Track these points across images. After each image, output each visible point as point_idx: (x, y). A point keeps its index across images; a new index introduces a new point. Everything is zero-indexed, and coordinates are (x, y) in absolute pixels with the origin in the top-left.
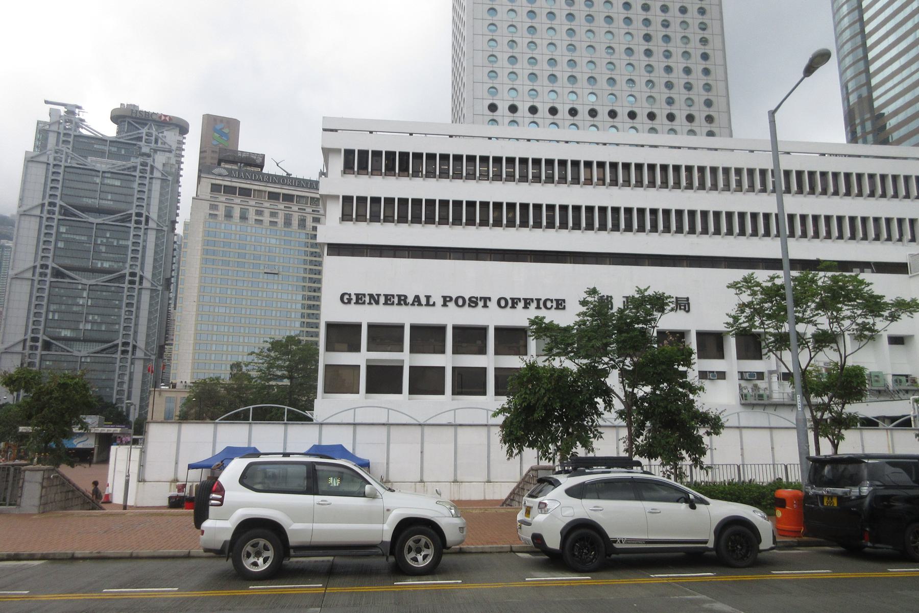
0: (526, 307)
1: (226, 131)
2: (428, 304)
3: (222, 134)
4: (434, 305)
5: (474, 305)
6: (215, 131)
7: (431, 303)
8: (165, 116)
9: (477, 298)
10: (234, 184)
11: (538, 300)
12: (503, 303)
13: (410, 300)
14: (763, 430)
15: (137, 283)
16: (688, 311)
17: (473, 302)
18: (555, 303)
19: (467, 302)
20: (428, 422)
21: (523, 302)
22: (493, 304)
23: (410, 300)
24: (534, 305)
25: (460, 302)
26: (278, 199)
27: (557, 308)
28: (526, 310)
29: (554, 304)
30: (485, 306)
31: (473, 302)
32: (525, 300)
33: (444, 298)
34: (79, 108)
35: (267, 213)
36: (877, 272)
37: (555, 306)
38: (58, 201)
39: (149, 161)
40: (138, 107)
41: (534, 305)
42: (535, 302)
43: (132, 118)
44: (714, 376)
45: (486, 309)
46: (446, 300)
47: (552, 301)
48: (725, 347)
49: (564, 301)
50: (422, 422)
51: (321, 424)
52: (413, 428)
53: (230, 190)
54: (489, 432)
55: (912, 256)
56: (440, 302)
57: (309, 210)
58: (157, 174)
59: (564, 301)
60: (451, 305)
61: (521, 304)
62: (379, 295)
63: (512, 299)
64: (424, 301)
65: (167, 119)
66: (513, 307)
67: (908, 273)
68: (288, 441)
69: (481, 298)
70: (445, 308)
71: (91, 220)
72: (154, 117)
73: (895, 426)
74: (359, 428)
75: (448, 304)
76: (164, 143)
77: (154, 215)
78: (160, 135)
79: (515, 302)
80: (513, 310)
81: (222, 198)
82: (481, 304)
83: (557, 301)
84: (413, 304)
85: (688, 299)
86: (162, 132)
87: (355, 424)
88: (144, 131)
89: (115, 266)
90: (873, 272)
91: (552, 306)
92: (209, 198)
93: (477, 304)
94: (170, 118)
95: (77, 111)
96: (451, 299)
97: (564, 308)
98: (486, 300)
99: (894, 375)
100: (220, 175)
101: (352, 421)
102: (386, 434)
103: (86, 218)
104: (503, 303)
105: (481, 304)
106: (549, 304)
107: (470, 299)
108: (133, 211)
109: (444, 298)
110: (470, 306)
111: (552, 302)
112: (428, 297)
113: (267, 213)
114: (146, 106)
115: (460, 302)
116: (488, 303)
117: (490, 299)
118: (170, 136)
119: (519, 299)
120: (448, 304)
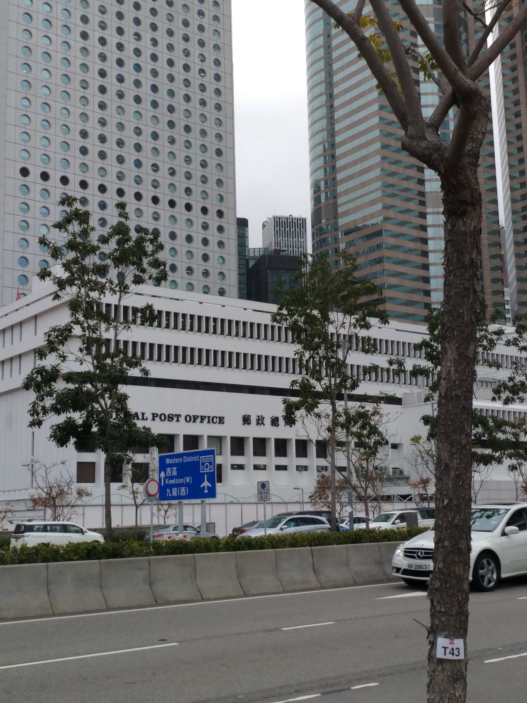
0: (201, 422)
2: (143, 419)
4: (147, 419)
5: (171, 420)
7: (145, 418)
9: (173, 415)
11: (209, 417)
12: (188, 419)
14: (281, 504)
17: (170, 418)
18: (218, 419)
19: (167, 418)
20: (289, 501)
21: (200, 418)
22: (182, 419)
24: (206, 420)
25: (163, 418)
27: (220, 423)
28: (202, 424)
29: (218, 420)
30: (178, 421)
31: (170, 418)
32: (201, 417)
33: (153, 414)
36: (387, 403)
37: (218, 422)
41: (206, 420)
42: (207, 418)
44: (302, 469)
45: (178, 423)
46: (154, 416)
47: (216, 418)
48: (308, 449)
49: (223, 418)
50: (286, 501)
51: (242, 503)
52: (188, 506)
54: (272, 506)
55: (405, 394)
56: (150, 417)
59: (223, 418)
60: (157, 419)
61: (199, 420)
63: (194, 416)
64: (140, 416)
66: (194, 421)
67: (401, 405)
68: (124, 516)
69: (175, 415)
70: (154, 421)
73: (408, 500)
74: (124, 508)
75: (155, 418)
79: (195, 418)
80: (194, 424)
82: (175, 419)
83: (220, 418)
87: (122, 505)
90: (385, 403)
93: (173, 419)
96: (157, 415)
97: (223, 423)
98: (178, 416)
99: (393, 468)
101: (120, 503)
102: (120, 511)
104: (188, 419)
105: (175, 419)
106: (215, 420)
107: (169, 415)
109: (153, 414)
110: (169, 420)
112: (143, 414)
115: (163, 418)
116: (180, 419)
117: (180, 416)
119: (198, 416)
120: (155, 418)
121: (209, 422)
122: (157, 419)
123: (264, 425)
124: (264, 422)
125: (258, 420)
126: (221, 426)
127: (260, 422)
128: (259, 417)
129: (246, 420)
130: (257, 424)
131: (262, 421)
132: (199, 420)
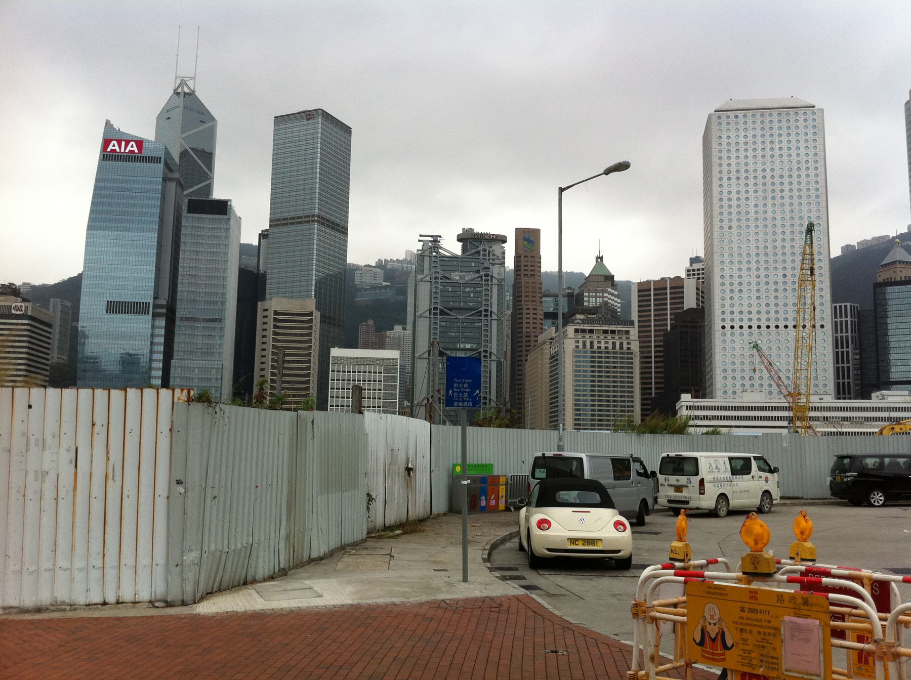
1: (532, 239)
3: (529, 241)
6: (525, 239)
8: (493, 235)
10: (585, 328)
15: (489, 357)
26: (607, 333)
34: (440, 237)
35: (603, 342)
38: (439, 307)
39: (490, 273)
40: (472, 230)
43: (471, 239)
53: (584, 331)
57: (624, 338)
58: (495, 281)
65: (494, 237)
71: (458, 317)
72: (486, 237)
76: (494, 255)
77: (495, 309)
78: (491, 250)
81: (580, 336)
86: (491, 247)
88: (481, 248)
89: (475, 346)
92: (573, 337)
94: (497, 236)
95: (439, 239)
100: (578, 323)
103: (454, 316)
108: (483, 309)
113: (603, 342)
114: (479, 229)
118: (496, 248)
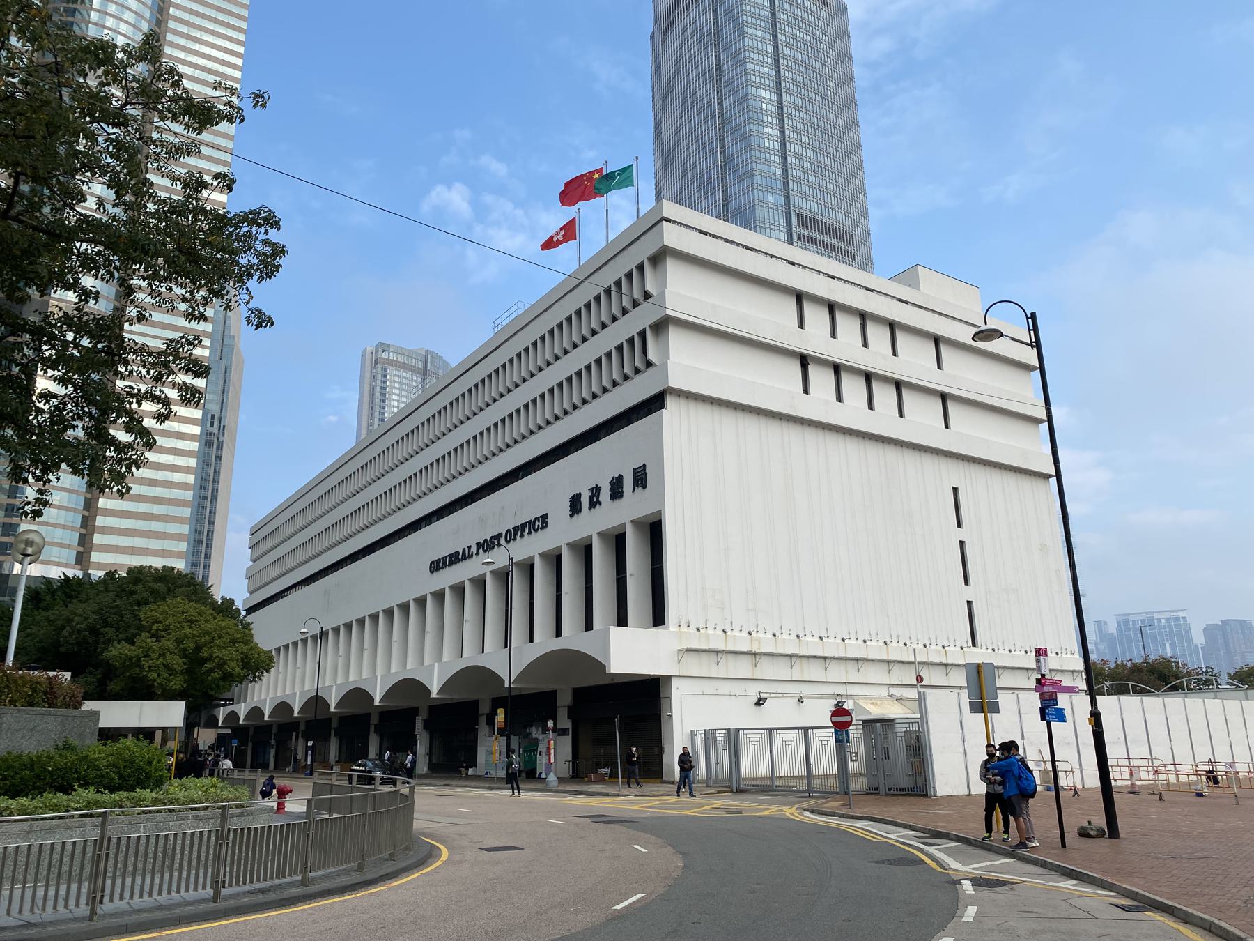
0: (522, 536)
4: (472, 556)
11: (530, 522)
13: (460, 557)
16: (644, 487)
23: (460, 557)
30: (499, 545)
46: (479, 545)
60: (481, 551)
61: (519, 533)
62: (446, 557)
66: (515, 539)
79: (516, 529)
84: (462, 560)
85: (644, 465)
91: (538, 525)
93: (494, 543)
98: (499, 536)
106: (537, 523)
111: (539, 521)
117: (500, 535)
121: (530, 533)
122: (481, 551)
123: (600, 504)
124: (600, 499)
125: (591, 498)
126: (545, 531)
127: (595, 500)
128: (591, 490)
129: (575, 505)
130: (590, 509)
131: (598, 498)
132: (519, 533)
